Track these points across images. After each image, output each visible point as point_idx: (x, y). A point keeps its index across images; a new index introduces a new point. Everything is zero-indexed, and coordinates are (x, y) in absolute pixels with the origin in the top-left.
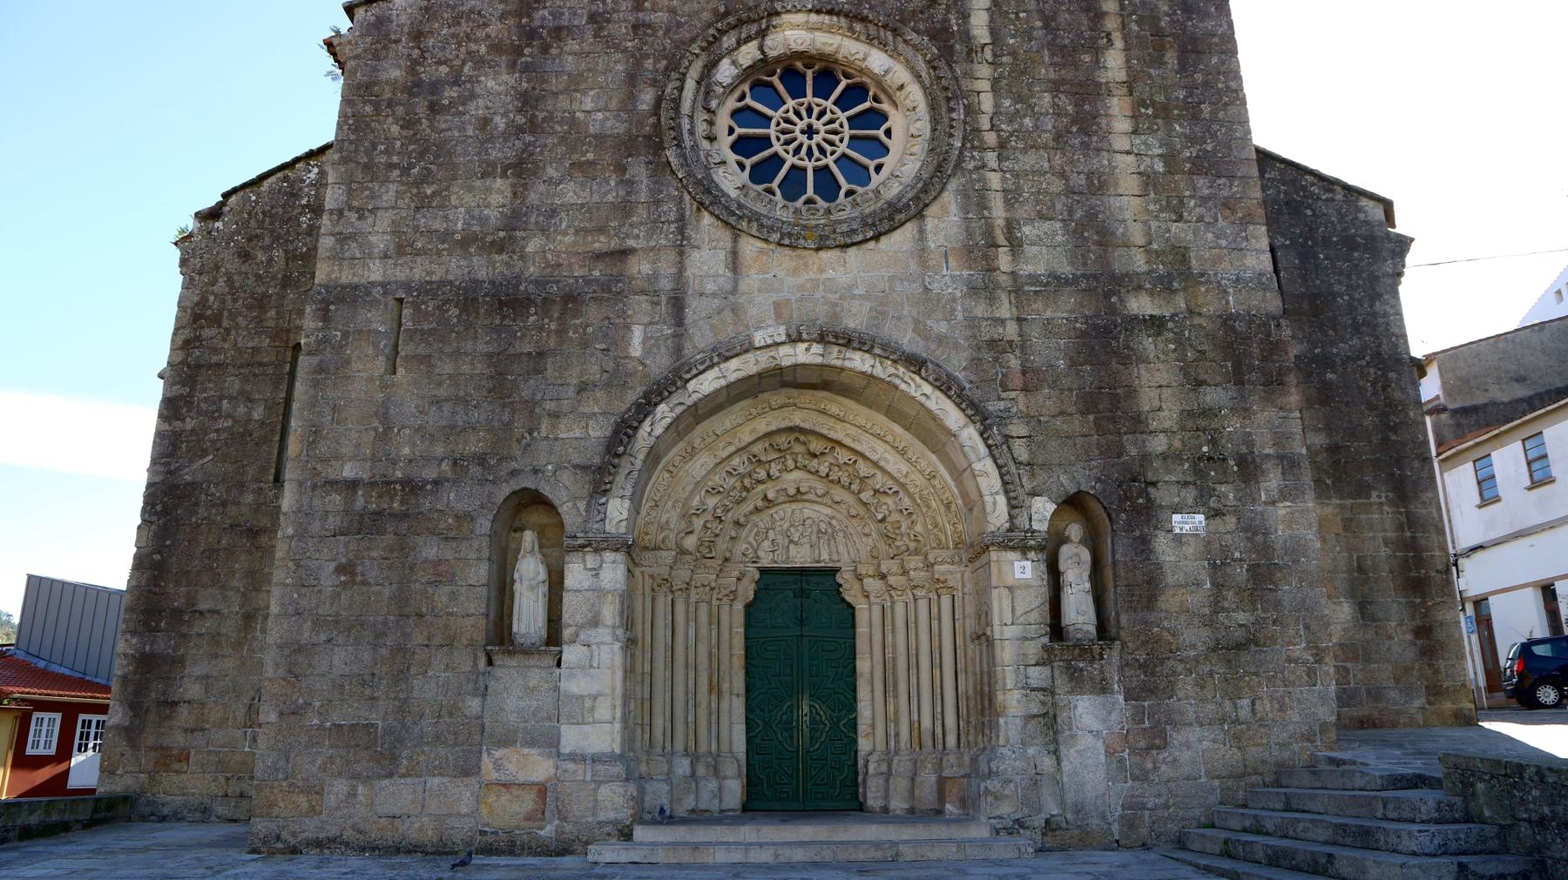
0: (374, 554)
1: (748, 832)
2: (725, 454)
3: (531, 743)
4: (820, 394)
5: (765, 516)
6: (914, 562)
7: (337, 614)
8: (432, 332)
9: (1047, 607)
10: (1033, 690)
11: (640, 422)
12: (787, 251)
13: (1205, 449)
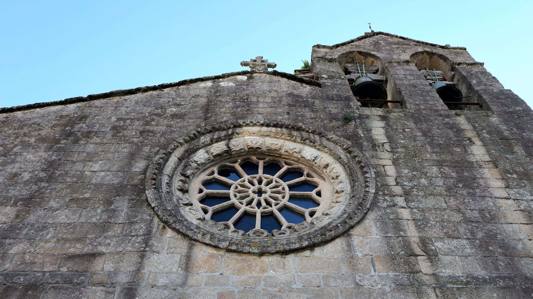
12: (235, 256)
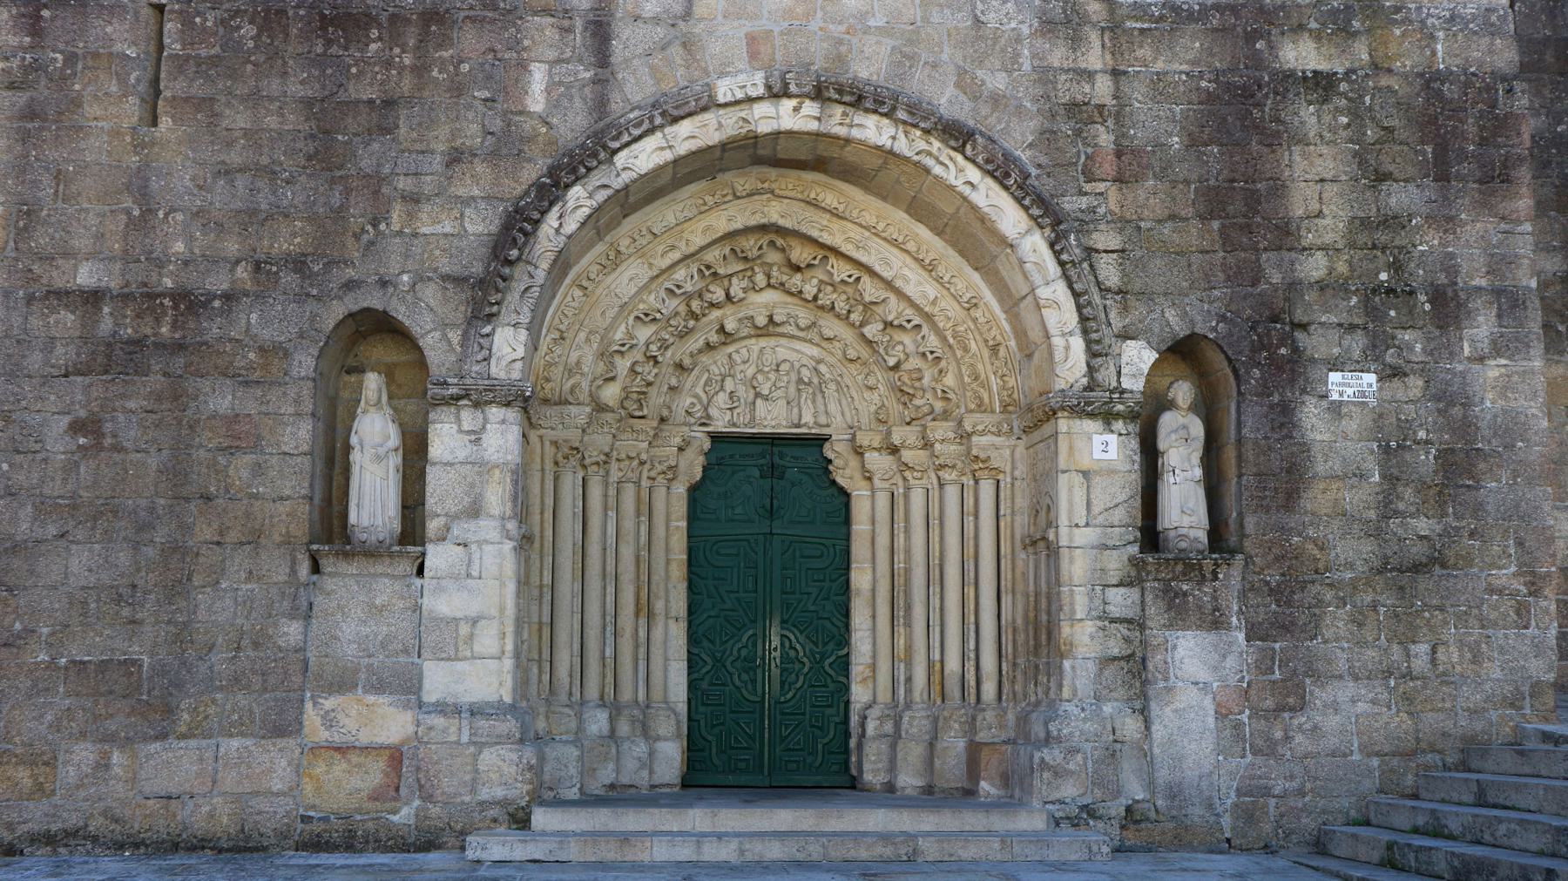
0: (132, 405)
1: (697, 818)
2: (667, 262)
3: (379, 687)
4: (809, 176)
5: (721, 356)
6: (941, 430)
7: (74, 495)
8: (214, 61)
9: (1138, 502)
10: (1113, 621)
11: (544, 213)
13: (1383, 276)
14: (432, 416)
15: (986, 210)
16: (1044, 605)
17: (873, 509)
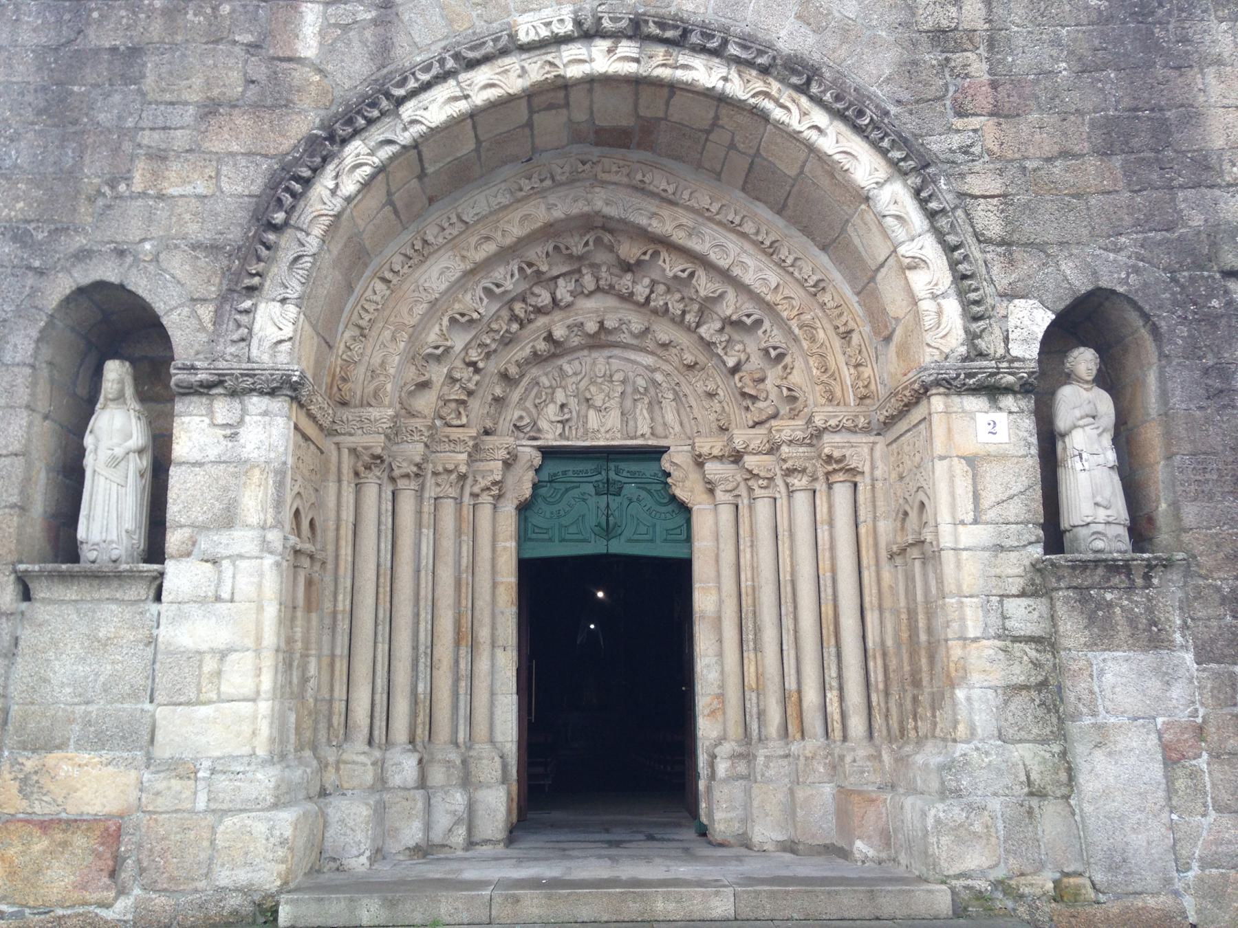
2: (480, 256)
6: (788, 429)
9: (1038, 493)
10: (1016, 639)
14: (179, 406)
15: (837, 157)
16: (922, 624)
17: (716, 524)
